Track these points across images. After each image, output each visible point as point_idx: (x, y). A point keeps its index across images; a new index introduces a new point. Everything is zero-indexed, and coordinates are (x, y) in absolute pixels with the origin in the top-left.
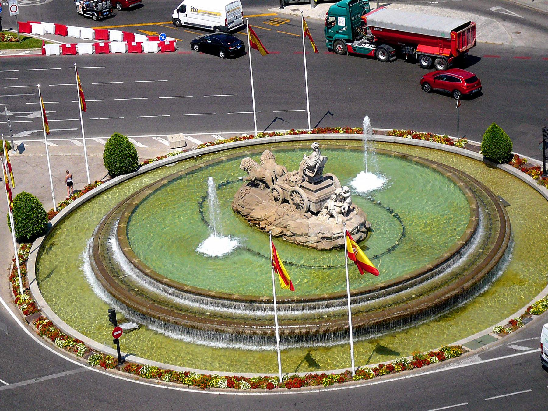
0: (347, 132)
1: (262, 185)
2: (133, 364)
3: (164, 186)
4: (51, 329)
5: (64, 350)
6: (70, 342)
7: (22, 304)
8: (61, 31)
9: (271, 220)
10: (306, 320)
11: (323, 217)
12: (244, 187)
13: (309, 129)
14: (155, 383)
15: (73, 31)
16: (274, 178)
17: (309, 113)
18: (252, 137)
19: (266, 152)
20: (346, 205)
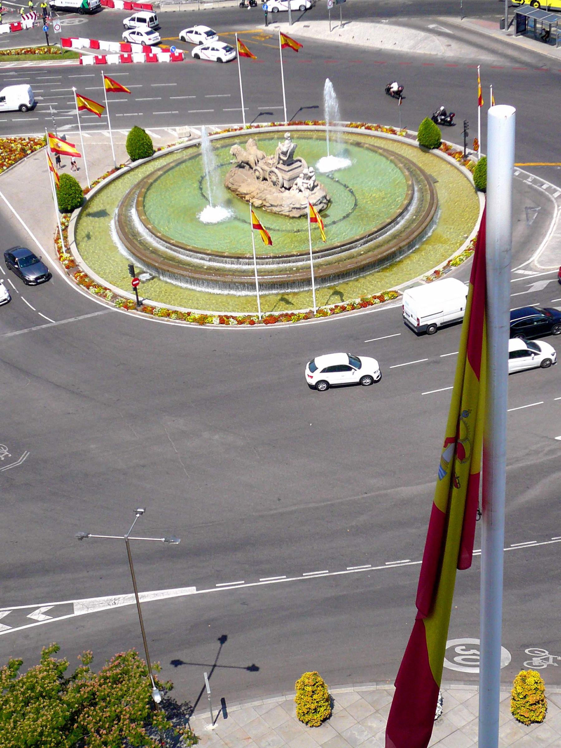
0: (315, 124)
1: (247, 167)
2: (148, 306)
3: (172, 168)
4: (87, 280)
5: (96, 296)
6: (100, 290)
7: (64, 261)
8: (95, 45)
9: (254, 194)
10: (281, 271)
11: (294, 192)
12: (233, 168)
13: (286, 122)
14: (165, 321)
15: (104, 45)
16: (257, 161)
17: (285, 110)
18: (241, 128)
19: (250, 140)
20: (311, 182)
